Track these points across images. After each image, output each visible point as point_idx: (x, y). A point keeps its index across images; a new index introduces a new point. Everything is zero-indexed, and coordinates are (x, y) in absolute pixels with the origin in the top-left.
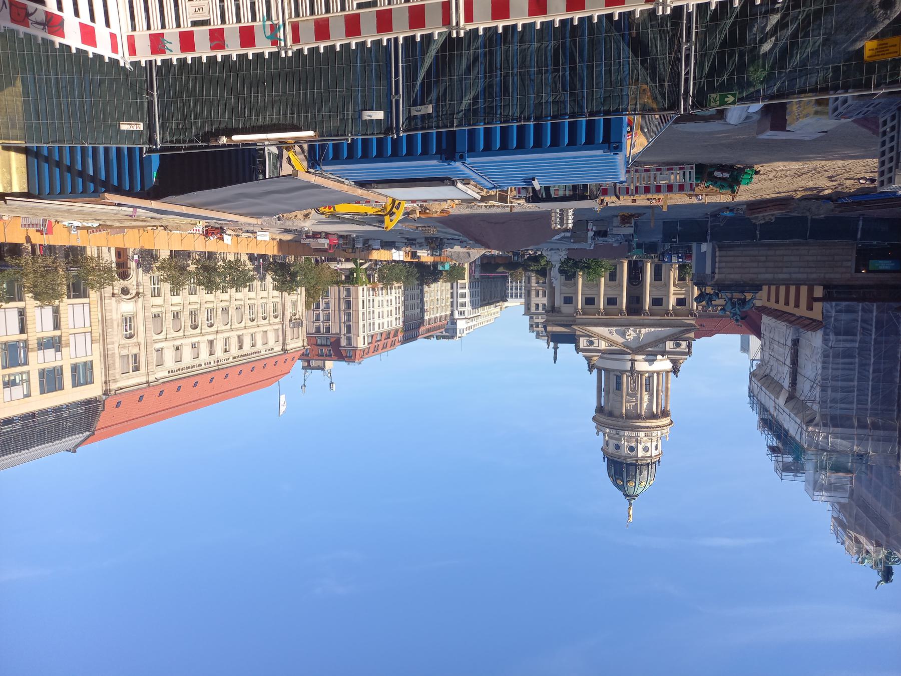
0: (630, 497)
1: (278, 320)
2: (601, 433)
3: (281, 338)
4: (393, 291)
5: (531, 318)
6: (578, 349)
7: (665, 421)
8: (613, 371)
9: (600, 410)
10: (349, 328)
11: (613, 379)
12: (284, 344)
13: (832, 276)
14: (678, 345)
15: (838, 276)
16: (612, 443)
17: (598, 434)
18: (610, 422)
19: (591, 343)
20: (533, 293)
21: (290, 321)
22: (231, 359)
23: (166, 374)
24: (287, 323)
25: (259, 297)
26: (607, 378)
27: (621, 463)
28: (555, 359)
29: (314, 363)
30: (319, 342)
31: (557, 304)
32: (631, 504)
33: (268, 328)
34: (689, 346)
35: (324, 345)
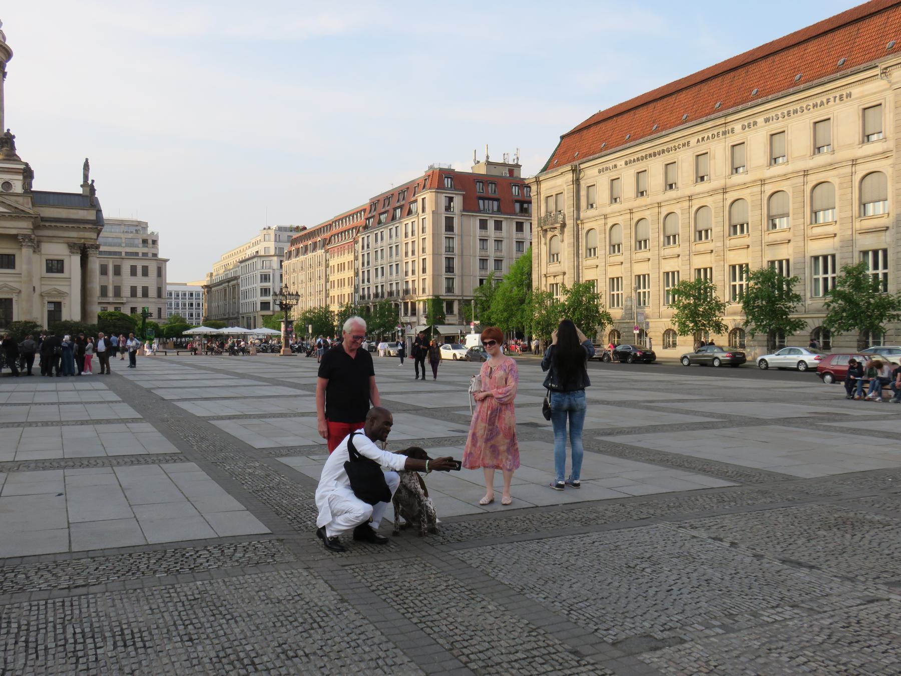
1: (587, 226)
3: (583, 193)
4: (373, 291)
5: (155, 255)
6: (28, 173)
10: (449, 227)
12: (577, 182)
20: (152, 292)
21: (564, 225)
22: (693, 141)
23: (856, 91)
24: (570, 223)
25: (627, 265)
28: (86, 166)
29: (505, 172)
30: (495, 203)
31: (76, 260)
33: (608, 210)
35: (489, 199)
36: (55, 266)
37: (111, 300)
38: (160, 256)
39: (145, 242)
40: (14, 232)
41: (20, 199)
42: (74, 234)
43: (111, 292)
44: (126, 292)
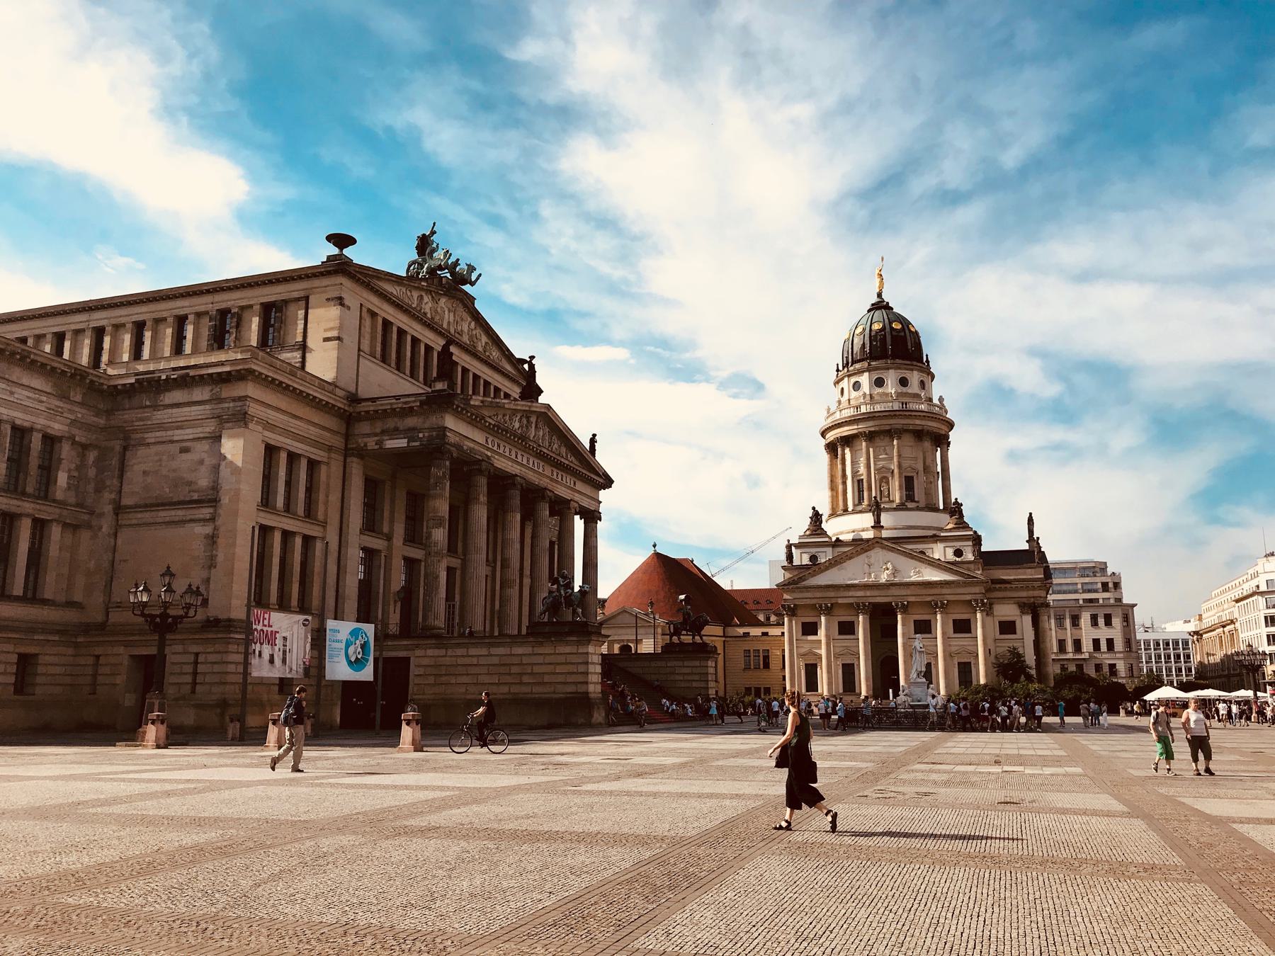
0: (880, 305)
2: (936, 401)
5: (1119, 600)
6: (977, 540)
7: (831, 436)
8: (918, 509)
9: (942, 441)
11: (919, 493)
13: (437, 652)
14: (813, 558)
15: (430, 652)
16: (914, 387)
17: (941, 399)
18: (918, 422)
19: (958, 553)
20: (1119, 645)
26: (930, 493)
27: (894, 357)
31: (1027, 619)
32: (879, 295)
34: (790, 557)
36: (1008, 627)
37: (1070, 656)
38: (1125, 601)
39: (1105, 585)
40: (968, 598)
41: (972, 566)
42: (1024, 594)
43: (1070, 647)
44: (1087, 646)
